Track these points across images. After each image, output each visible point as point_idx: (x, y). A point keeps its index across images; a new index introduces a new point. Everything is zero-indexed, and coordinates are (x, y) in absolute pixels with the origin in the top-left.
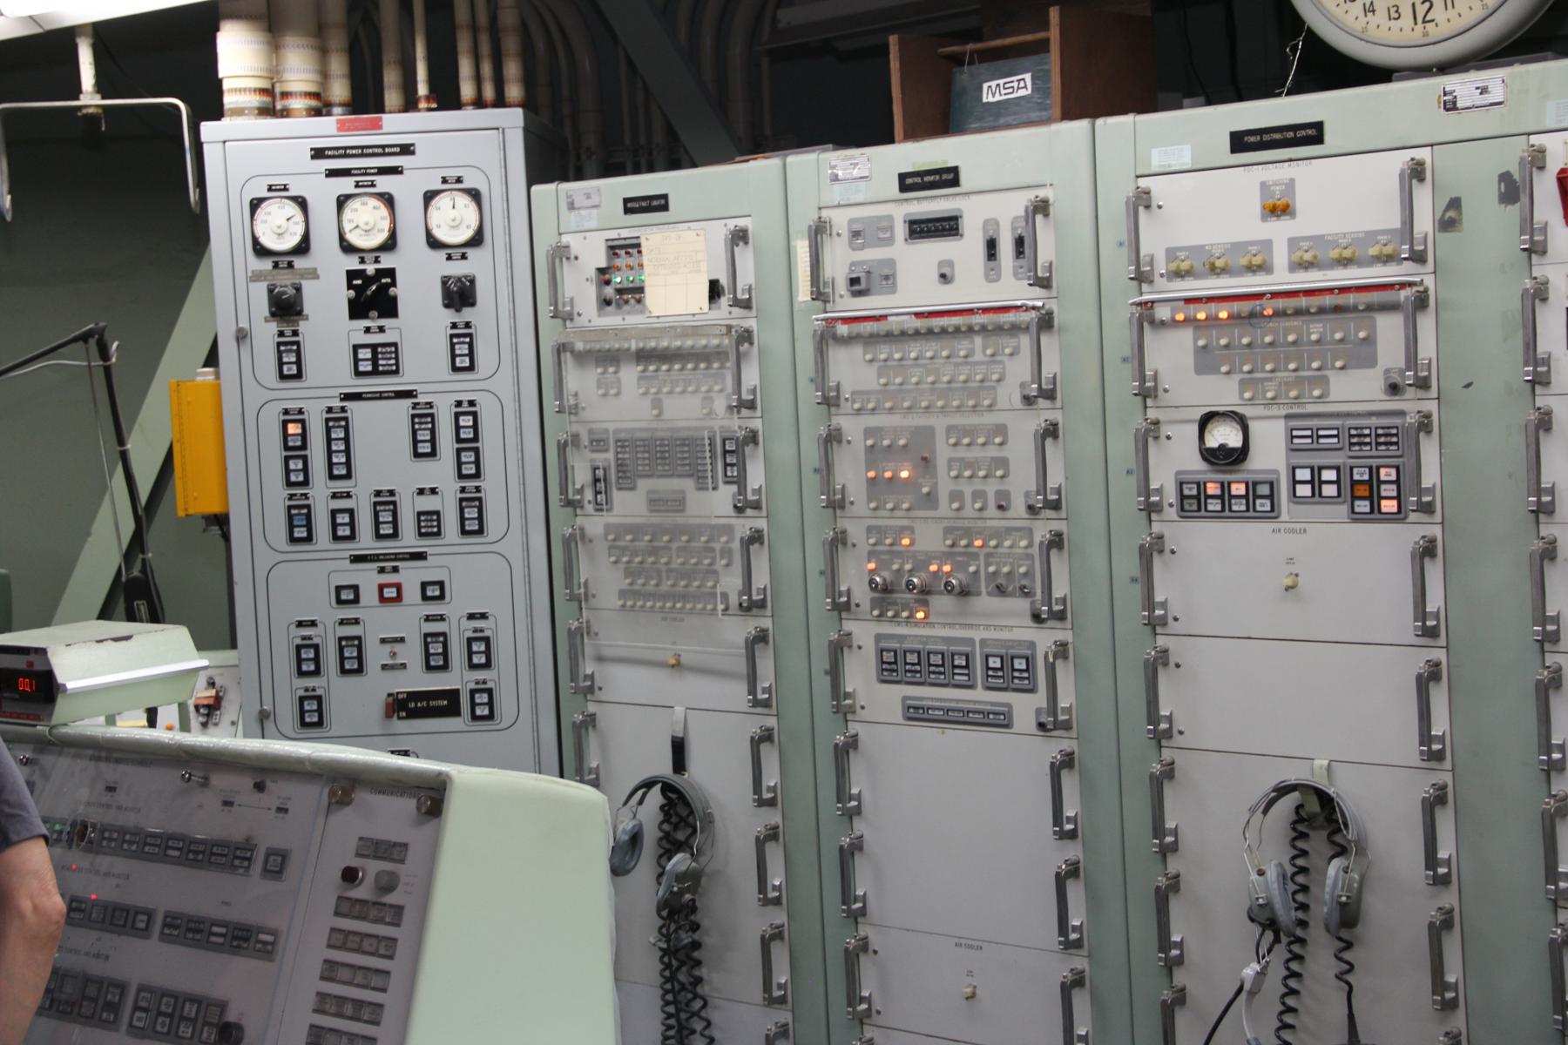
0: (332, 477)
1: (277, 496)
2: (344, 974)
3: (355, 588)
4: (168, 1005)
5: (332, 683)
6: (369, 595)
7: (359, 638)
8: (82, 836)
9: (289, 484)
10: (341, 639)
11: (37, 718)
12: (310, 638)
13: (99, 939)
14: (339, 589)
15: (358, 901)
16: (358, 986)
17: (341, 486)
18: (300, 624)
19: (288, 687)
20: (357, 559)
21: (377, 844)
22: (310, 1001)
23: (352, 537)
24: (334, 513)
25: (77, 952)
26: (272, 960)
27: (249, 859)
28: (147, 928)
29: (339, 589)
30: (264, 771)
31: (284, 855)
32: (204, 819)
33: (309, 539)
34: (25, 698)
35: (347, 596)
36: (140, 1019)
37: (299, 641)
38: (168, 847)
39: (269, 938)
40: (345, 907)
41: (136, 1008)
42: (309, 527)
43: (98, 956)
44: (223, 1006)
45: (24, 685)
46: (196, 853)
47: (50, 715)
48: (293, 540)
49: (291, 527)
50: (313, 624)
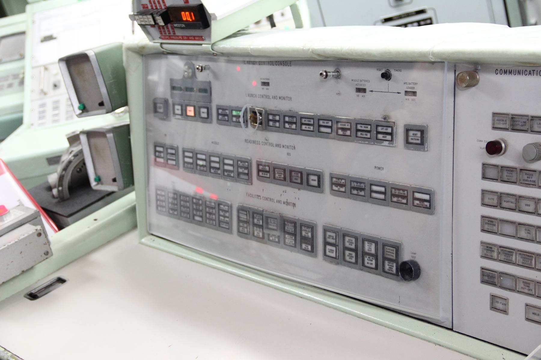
2: (509, 229)
4: (351, 243)
8: (254, 120)
11: (201, 38)
13: (285, 192)
15: (503, 168)
16: (521, 239)
21: (513, 118)
22: (477, 250)
25: (271, 200)
26: (432, 214)
27: (391, 134)
28: (319, 186)
30: (387, 67)
31: (423, 131)
32: (349, 107)
34: (189, 26)
36: (331, 251)
38: (320, 126)
39: (427, 197)
40: (491, 173)
41: (326, 243)
43: (287, 203)
44: (397, 248)
45: (186, 16)
46: (343, 129)
47: (209, 36)
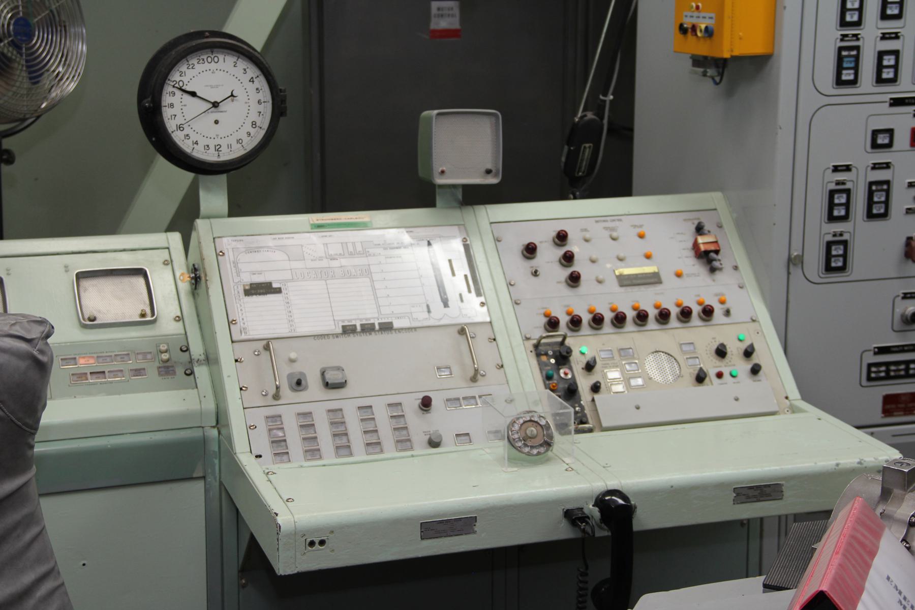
0: (884, 16)
1: (830, 36)
3: (890, 132)
5: (859, 229)
6: (902, 139)
7: (888, 182)
9: (843, 23)
10: (871, 184)
12: (843, 183)
14: (875, 133)
17: (891, 26)
18: (836, 169)
19: (820, 230)
20: (897, 102)
23: (893, 80)
24: (881, 55)
29: (875, 133)
33: (854, 82)
35: (881, 140)
37: (833, 186)
42: (856, 69)
48: (840, 82)
49: (840, 68)
50: (848, 168)
